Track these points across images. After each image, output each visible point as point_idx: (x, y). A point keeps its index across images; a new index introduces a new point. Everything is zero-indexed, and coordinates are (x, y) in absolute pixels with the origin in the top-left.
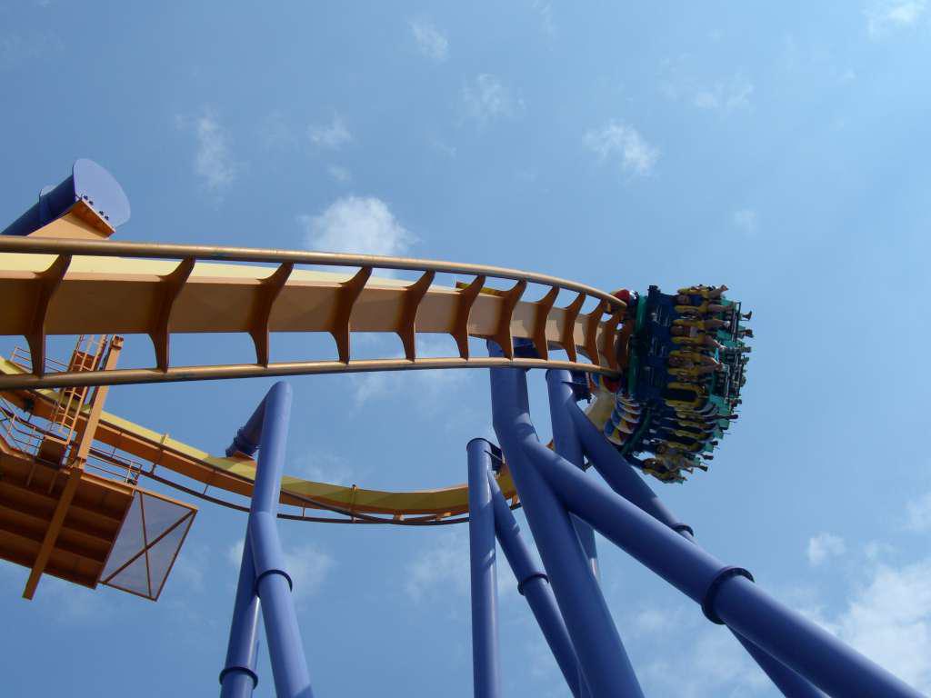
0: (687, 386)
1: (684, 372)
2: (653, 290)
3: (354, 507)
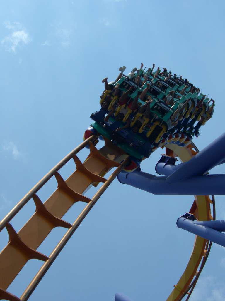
0: (152, 128)
1: (144, 125)
2: (93, 117)
3: (183, 291)
